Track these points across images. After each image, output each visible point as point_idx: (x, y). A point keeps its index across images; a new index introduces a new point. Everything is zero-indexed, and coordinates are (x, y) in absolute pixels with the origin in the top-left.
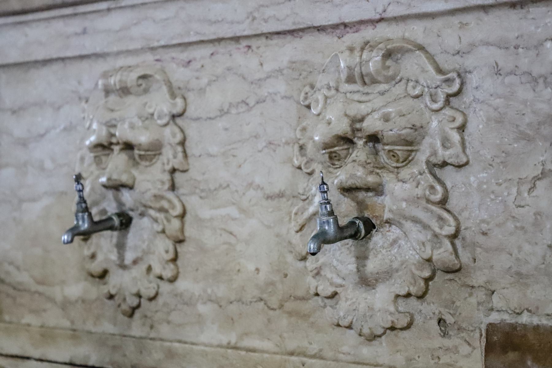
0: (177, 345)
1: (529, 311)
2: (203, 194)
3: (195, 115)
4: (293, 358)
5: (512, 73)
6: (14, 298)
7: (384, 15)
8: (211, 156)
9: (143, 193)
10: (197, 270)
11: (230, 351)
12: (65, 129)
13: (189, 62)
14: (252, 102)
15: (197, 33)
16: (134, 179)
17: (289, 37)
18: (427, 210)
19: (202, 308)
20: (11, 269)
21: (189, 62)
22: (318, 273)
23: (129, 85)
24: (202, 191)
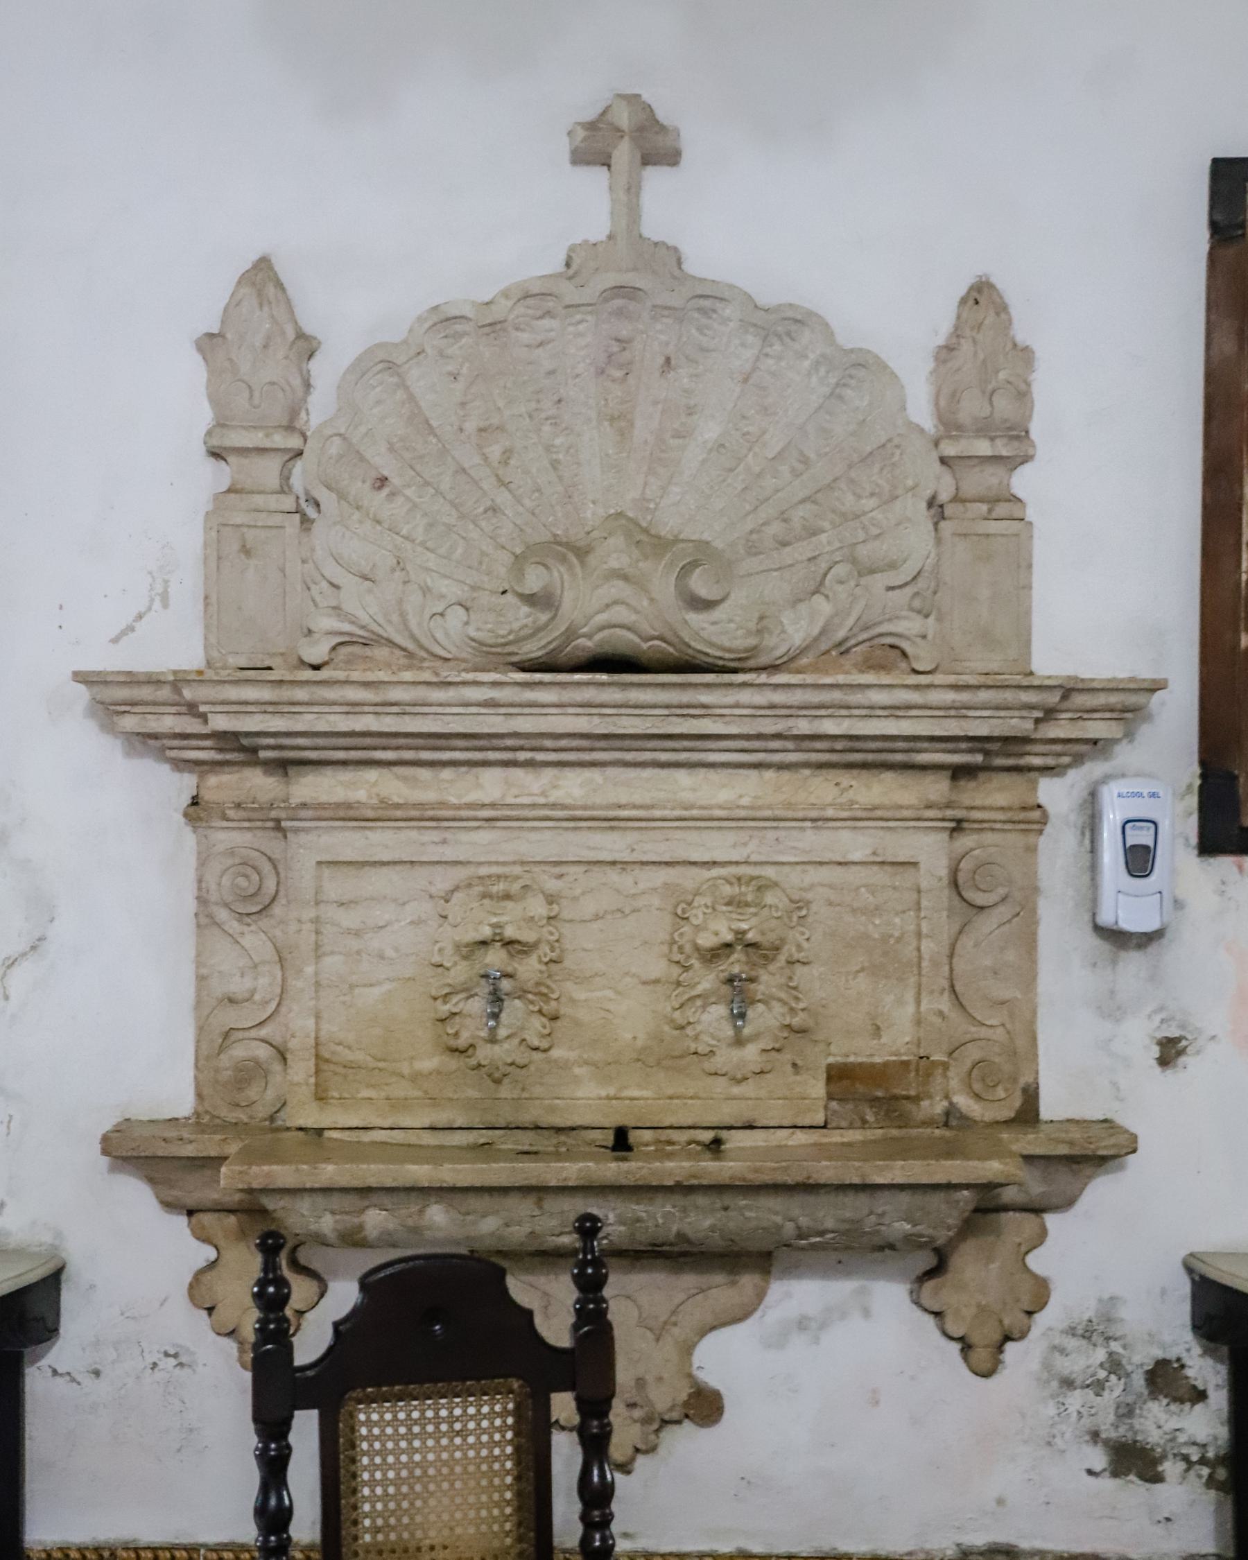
1: (855, 1054)
4: (676, 1101)
5: (839, 905)
6: (345, 1076)
7: (749, 860)
11: (614, 1101)
12: (412, 923)
13: (562, 875)
14: (627, 911)
16: (515, 969)
17: (663, 866)
18: (787, 992)
19: (577, 1071)
20: (340, 1048)
21: (562, 875)
22: (696, 1038)
24: (577, 978)
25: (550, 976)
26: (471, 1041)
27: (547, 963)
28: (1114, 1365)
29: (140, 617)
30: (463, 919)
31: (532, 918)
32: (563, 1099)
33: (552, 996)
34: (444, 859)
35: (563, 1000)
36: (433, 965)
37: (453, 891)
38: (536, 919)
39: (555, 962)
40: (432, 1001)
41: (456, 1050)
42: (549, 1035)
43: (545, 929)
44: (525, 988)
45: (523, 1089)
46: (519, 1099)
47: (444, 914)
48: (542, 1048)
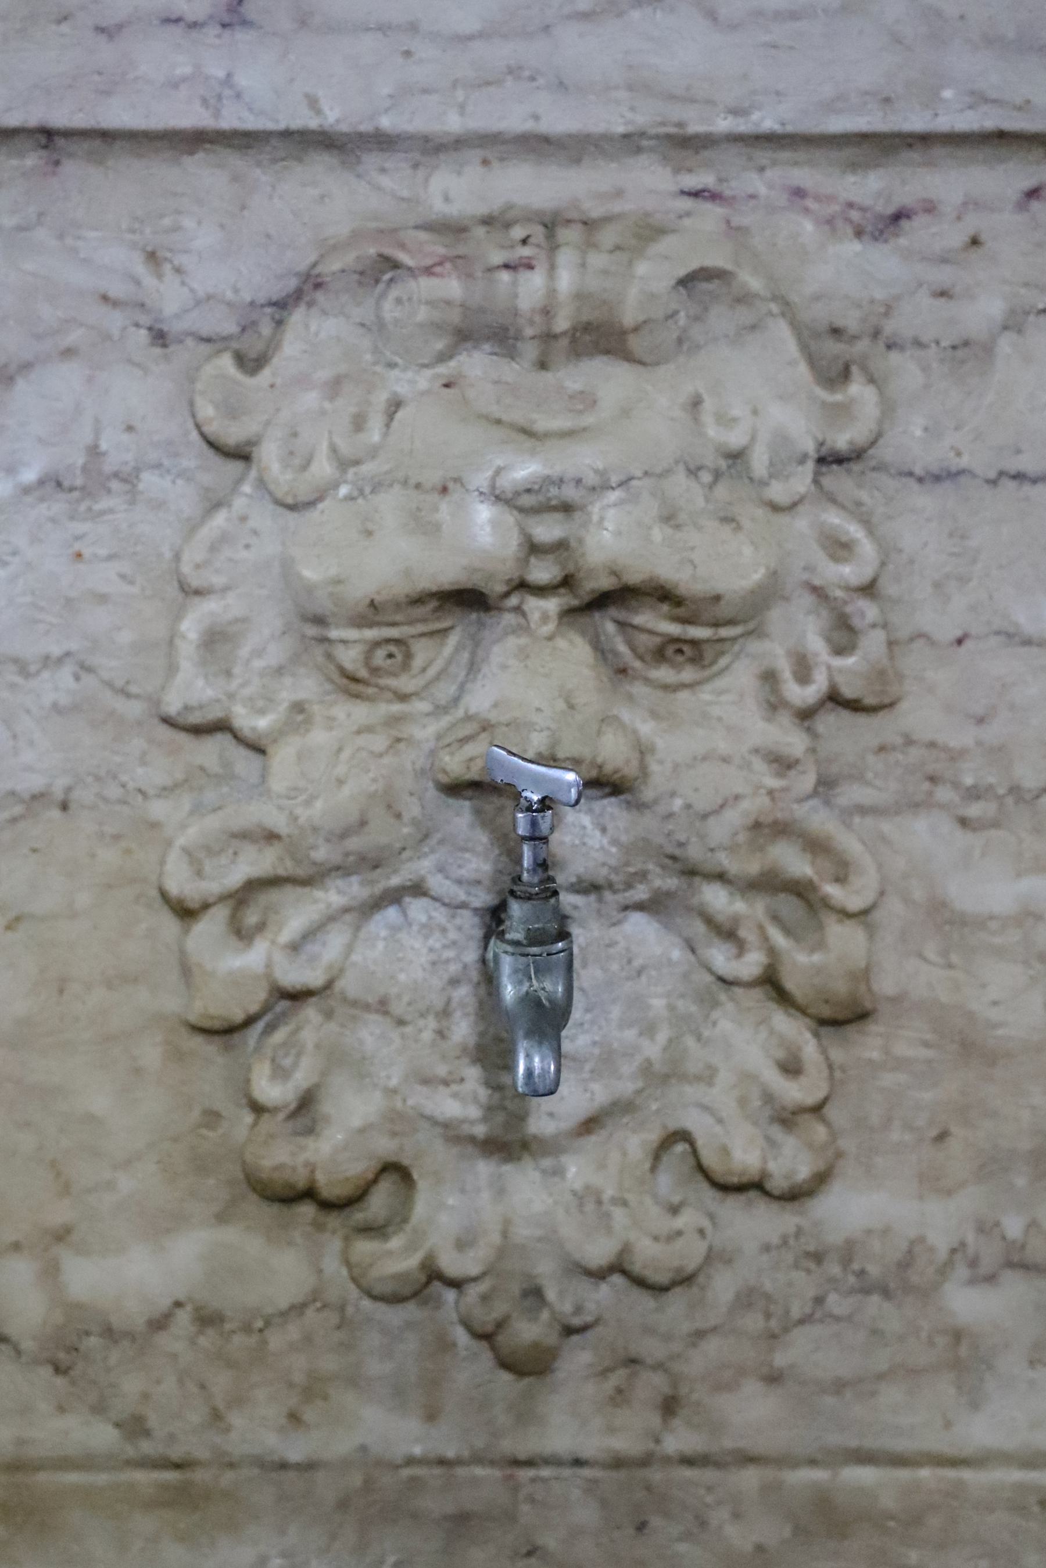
0: (865, 1475)
2: (974, 810)
3: (925, 459)
8: (1028, 642)
9: (705, 817)
10: (942, 1137)
13: (899, 217)
15: (979, 99)
16: (643, 750)
21: (899, 217)
23: (629, 318)
24: (974, 794)
25: (826, 785)
26: (385, 1147)
27: (806, 715)
30: (344, 464)
31: (736, 457)
32: (899, 1461)
33: (831, 890)
34: (231, 119)
35: (893, 910)
36: (167, 721)
37: (282, 305)
38: (759, 462)
39: (855, 706)
40: (169, 924)
41: (309, 1194)
42: (817, 1109)
43: (801, 523)
44: (695, 852)
45: (669, 1406)
46: (645, 1461)
47: (233, 434)
48: (778, 1184)
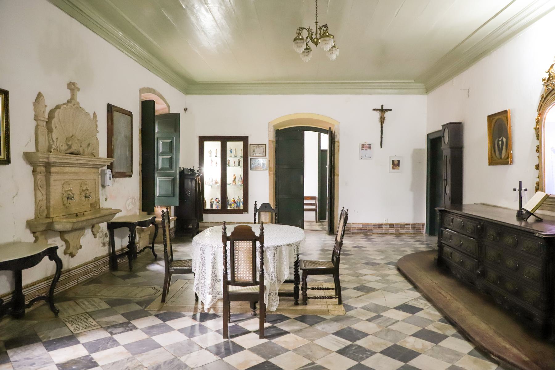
28: (103, 235)
29: (28, 143)
